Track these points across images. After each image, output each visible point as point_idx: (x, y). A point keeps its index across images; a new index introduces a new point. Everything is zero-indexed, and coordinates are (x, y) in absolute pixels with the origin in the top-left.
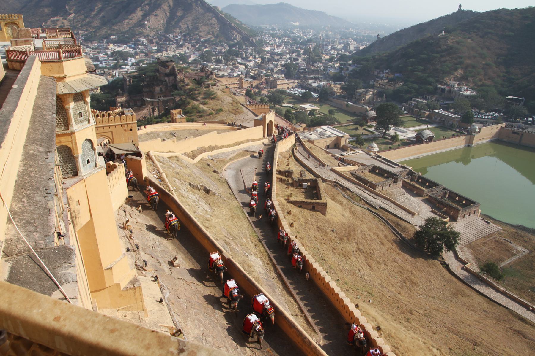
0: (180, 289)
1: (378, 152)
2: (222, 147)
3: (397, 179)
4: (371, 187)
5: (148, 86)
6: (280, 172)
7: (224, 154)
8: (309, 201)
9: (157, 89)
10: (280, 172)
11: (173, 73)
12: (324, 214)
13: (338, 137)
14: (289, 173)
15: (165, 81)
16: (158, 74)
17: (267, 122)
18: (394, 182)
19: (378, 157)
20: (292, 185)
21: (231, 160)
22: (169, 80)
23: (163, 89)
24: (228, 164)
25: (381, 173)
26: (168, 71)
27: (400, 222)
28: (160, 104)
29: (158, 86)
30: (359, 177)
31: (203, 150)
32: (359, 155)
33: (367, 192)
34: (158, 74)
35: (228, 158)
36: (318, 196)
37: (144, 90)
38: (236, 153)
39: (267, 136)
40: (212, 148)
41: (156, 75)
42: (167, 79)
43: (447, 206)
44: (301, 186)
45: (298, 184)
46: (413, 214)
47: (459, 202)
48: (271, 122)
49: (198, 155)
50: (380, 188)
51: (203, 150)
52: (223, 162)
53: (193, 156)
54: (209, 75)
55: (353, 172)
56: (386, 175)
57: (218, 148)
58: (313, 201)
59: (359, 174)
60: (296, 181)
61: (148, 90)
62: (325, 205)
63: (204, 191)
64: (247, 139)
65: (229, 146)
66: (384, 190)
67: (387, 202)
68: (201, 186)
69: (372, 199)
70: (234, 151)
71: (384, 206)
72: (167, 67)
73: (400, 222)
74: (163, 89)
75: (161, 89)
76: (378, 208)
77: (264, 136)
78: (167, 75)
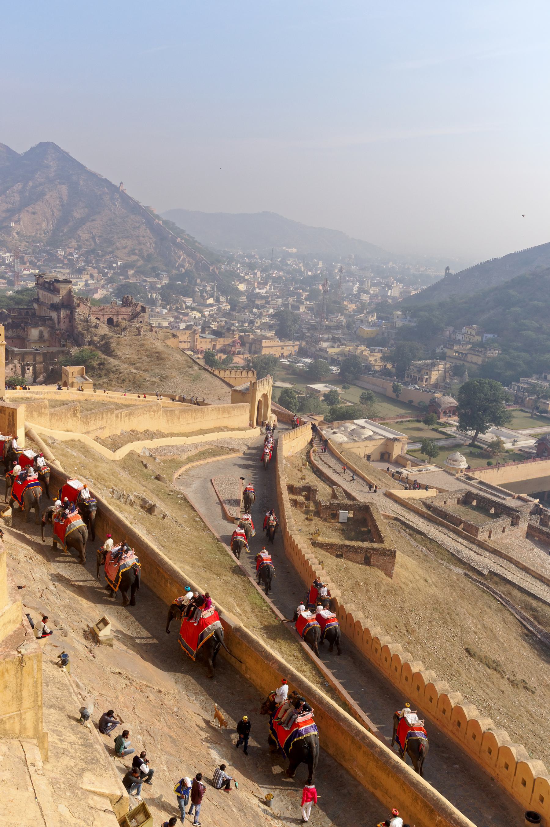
0: (122, 699)
1: (468, 469)
2: (171, 435)
3: (518, 517)
4: (469, 533)
6: (291, 489)
7: (177, 448)
9: (34, 333)
10: (291, 489)
11: (68, 304)
12: (389, 574)
13: (388, 439)
14: (309, 492)
15: (51, 319)
16: (36, 306)
18: (513, 524)
20: (317, 514)
21: (190, 460)
22: (59, 316)
23: (46, 335)
24: (184, 469)
26: (57, 299)
27: (534, 603)
28: (39, 358)
29: (36, 327)
30: (442, 511)
31: (134, 436)
32: (430, 472)
33: (460, 540)
34: (36, 306)
35: (185, 457)
36: (374, 534)
38: (200, 449)
39: (258, 424)
40: (150, 435)
41: (33, 309)
42: (54, 315)
44: (335, 516)
45: (329, 513)
48: (265, 396)
49: (123, 445)
51: (134, 436)
52: (175, 464)
53: (115, 447)
54: (138, 314)
55: (429, 502)
56: (493, 510)
57: (162, 435)
58: (365, 545)
59: (439, 504)
60: (326, 507)
62: (392, 554)
63: (142, 507)
64: (217, 425)
65: (187, 435)
66: (492, 538)
67: (501, 561)
68: (137, 497)
69: (472, 555)
70: (196, 446)
72: (56, 291)
73: (534, 603)
75: (41, 333)
76: (485, 572)
77: (251, 425)
78: (55, 307)
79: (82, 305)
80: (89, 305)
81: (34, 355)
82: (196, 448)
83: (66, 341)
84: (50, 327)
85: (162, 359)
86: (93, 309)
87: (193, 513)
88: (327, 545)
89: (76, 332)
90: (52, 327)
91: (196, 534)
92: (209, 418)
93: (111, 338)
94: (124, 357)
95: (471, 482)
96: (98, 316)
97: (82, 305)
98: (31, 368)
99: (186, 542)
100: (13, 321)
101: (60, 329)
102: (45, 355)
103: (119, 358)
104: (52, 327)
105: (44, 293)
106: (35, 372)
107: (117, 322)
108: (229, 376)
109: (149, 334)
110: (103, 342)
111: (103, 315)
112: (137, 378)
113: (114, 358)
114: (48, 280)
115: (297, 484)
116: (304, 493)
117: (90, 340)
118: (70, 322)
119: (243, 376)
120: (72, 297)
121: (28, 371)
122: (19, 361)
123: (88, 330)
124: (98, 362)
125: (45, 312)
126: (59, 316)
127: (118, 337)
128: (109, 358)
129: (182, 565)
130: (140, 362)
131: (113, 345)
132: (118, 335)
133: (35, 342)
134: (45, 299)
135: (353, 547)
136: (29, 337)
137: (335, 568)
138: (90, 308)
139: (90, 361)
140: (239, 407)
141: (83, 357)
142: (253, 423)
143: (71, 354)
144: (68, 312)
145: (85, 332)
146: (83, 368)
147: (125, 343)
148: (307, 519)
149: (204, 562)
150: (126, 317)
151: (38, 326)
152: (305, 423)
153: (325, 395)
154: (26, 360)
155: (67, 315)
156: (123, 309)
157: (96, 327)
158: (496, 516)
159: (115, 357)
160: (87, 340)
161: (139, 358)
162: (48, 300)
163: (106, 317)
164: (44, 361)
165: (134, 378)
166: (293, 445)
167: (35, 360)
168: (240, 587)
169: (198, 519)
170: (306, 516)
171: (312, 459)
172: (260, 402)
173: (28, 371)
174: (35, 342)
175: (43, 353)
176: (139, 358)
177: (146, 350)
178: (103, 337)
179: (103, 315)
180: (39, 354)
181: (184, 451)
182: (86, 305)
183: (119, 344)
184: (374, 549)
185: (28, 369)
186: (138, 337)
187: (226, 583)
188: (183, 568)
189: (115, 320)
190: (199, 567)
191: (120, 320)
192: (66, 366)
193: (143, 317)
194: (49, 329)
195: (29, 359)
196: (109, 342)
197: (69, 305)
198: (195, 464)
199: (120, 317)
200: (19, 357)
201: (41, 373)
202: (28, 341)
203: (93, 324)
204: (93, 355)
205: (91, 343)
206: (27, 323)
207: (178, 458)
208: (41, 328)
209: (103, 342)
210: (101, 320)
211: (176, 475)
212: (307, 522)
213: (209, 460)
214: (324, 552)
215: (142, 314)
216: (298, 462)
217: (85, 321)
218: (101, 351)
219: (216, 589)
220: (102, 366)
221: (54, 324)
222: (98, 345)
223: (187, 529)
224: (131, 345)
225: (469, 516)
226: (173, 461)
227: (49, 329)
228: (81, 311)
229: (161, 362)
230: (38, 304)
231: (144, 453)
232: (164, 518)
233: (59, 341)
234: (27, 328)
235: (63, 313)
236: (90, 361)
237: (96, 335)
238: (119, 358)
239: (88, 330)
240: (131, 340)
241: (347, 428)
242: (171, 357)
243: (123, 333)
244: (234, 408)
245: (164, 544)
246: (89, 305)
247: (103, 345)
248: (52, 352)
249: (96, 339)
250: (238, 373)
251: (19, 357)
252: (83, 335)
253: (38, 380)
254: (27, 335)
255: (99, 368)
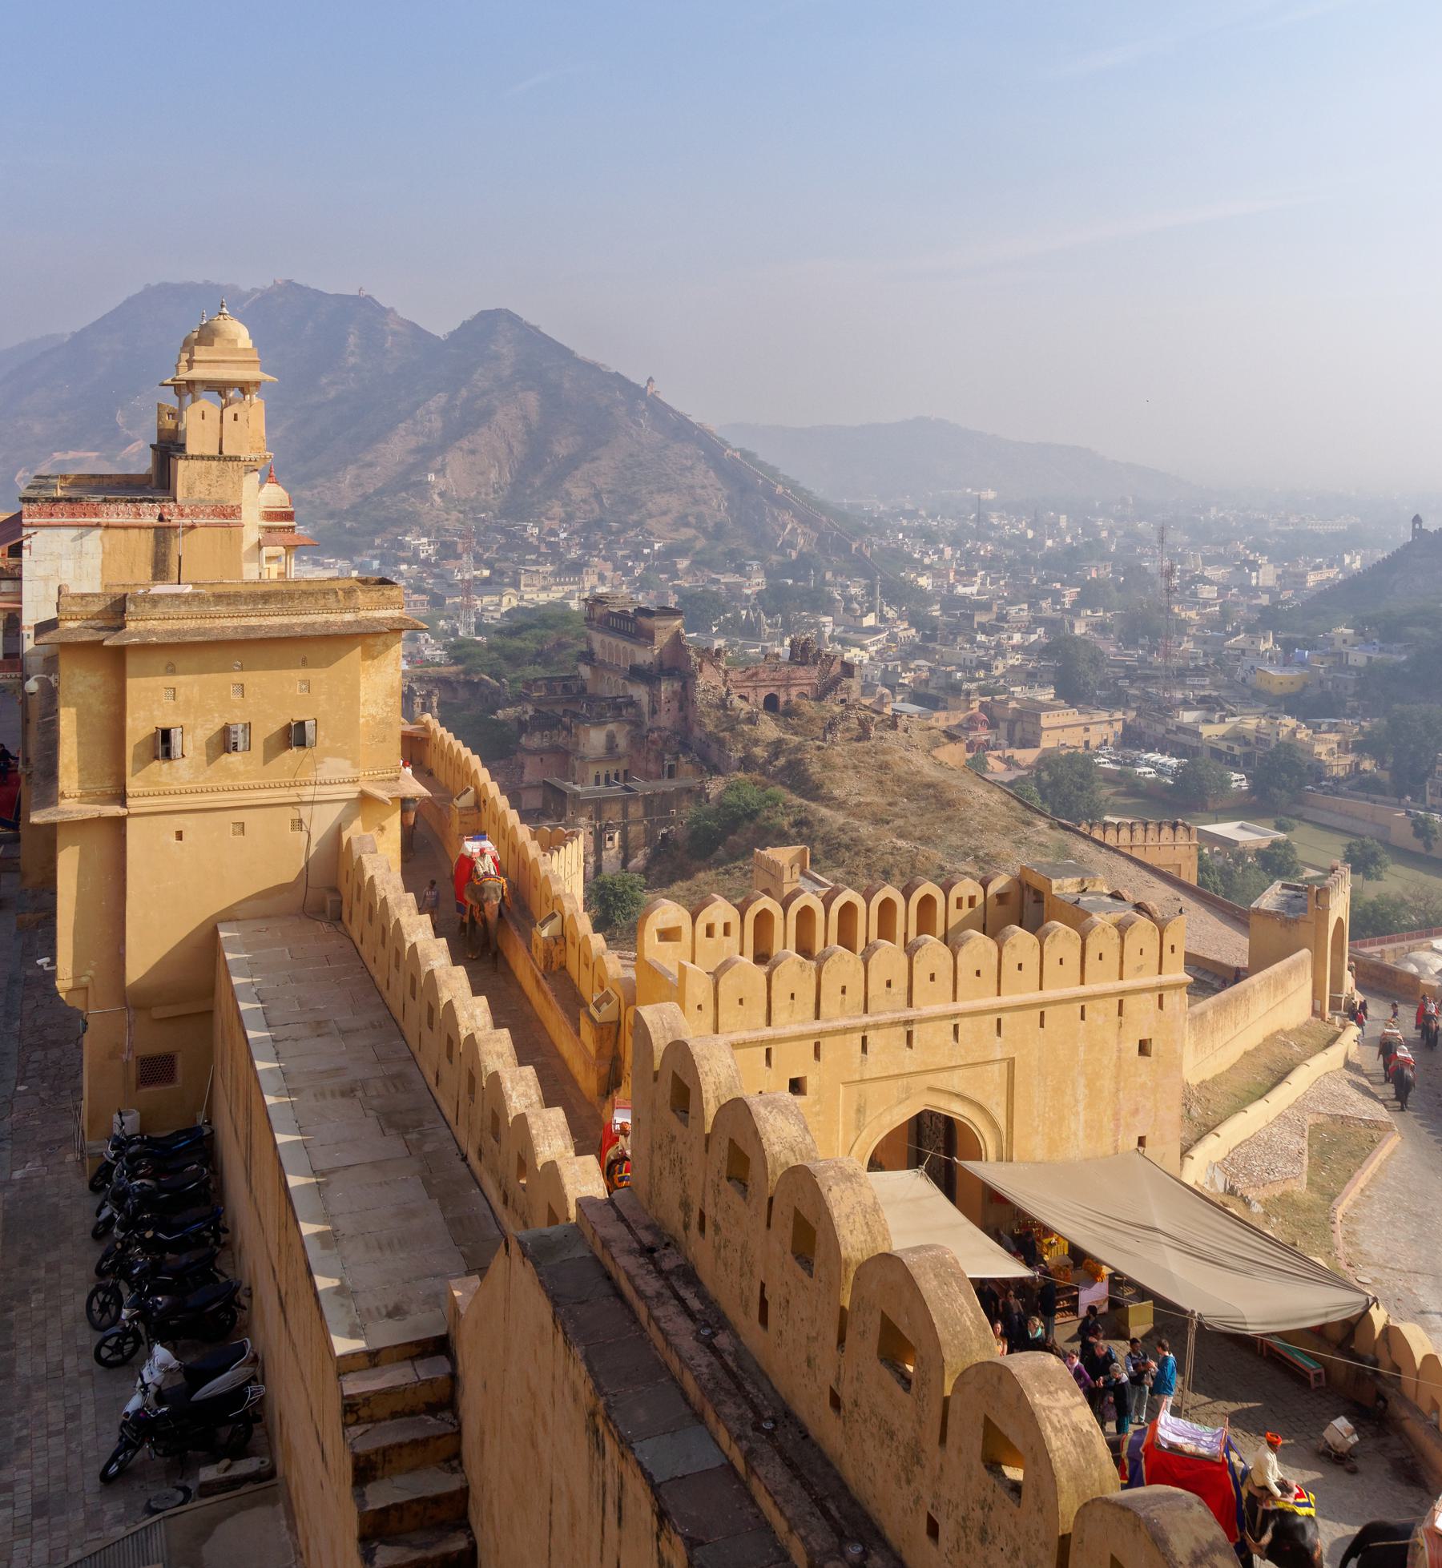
5: (544, 722)
9: (595, 739)
11: (676, 667)
15: (632, 703)
22: (654, 699)
23: (622, 742)
26: (645, 656)
28: (636, 810)
29: (600, 723)
34: (585, 671)
37: (535, 741)
42: (640, 693)
54: (836, 681)
61: (546, 744)
74: (622, 742)
75: (611, 738)
78: (637, 674)
79: (708, 669)
80: (723, 665)
81: (625, 802)
83: (677, 759)
84: (631, 722)
85: (950, 804)
86: (732, 675)
89: (697, 732)
90: (637, 724)
93: (799, 748)
94: (853, 800)
96: (743, 692)
97: (708, 669)
98: (617, 835)
100: (536, 711)
101: (659, 729)
102: (648, 801)
103: (840, 805)
104: (637, 724)
105: (608, 639)
106: (624, 845)
107: (788, 702)
108: (1127, 842)
109: (889, 735)
110: (781, 761)
111: (755, 688)
112: (918, 865)
113: (827, 806)
114: (616, 610)
117: (741, 754)
118: (681, 709)
119: (1164, 841)
120: (685, 648)
121: (609, 844)
122: (591, 818)
123: (732, 729)
124: (791, 819)
125: (611, 686)
126: (654, 699)
127: (819, 748)
128: (813, 805)
130: (896, 815)
131: (814, 768)
132: (818, 743)
133: (598, 761)
134: (611, 655)
136: (581, 748)
138: (726, 672)
139: (765, 813)
141: (747, 805)
142: (1322, 1007)
143: (708, 795)
144: (677, 686)
145: (727, 734)
146: (804, 851)
147: (839, 761)
150: (806, 689)
151: (605, 723)
153: (1259, 853)
154: (606, 816)
155: (674, 693)
156: (801, 672)
157: (752, 720)
159: (828, 800)
160: (736, 754)
161: (890, 804)
162: (618, 657)
163: (763, 693)
164: (646, 815)
165: (913, 867)
167: (625, 815)
173: (609, 844)
174: (598, 761)
175: (645, 797)
176: (890, 804)
177: (899, 780)
178: (777, 747)
179: (755, 688)
180: (636, 798)
182: (717, 667)
183: (827, 765)
185: (611, 839)
186: (867, 744)
189: (783, 699)
191: (793, 698)
192: (763, 849)
193: (849, 688)
194: (628, 728)
195: (613, 813)
196: (800, 762)
197: (676, 669)
199: (794, 692)
200: (590, 808)
201: (637, 848)
202: (582, 758)
203: (742, 715)
204: (770, 798)
205: (747, 763)
206: (575, 715)
208: (611, 727)
209: (781, 761)
210: (751, 699)
215: (846, 682)
217: (718, 707)
218: (783, 784)
220: (805, 830)
221: (640, 714)
222: (772, 769)
224: (855, 767)
227: (628, 728)
228: (708, 680)
229: (950, 812)
230: (594, 669)
231: (1212, 1182)
233: (660, 757)
234: (577, 728)
235: (666, 688)
236: (765, 813)
237: (756, 742)
238: (840, 805)
239: (732, 729)
240: (853, 753)
241: (1426, 965)
242: (969, 798)
243: (829, 736)
246: (723, 665)
247: (782, 769)
248: (664, 793)
249: (759, 752)
250: (1150, 834)
251: (590, 808)
252: (721, 743)
253: (632, 863)
254: (577, 744)
255: (799, 834)
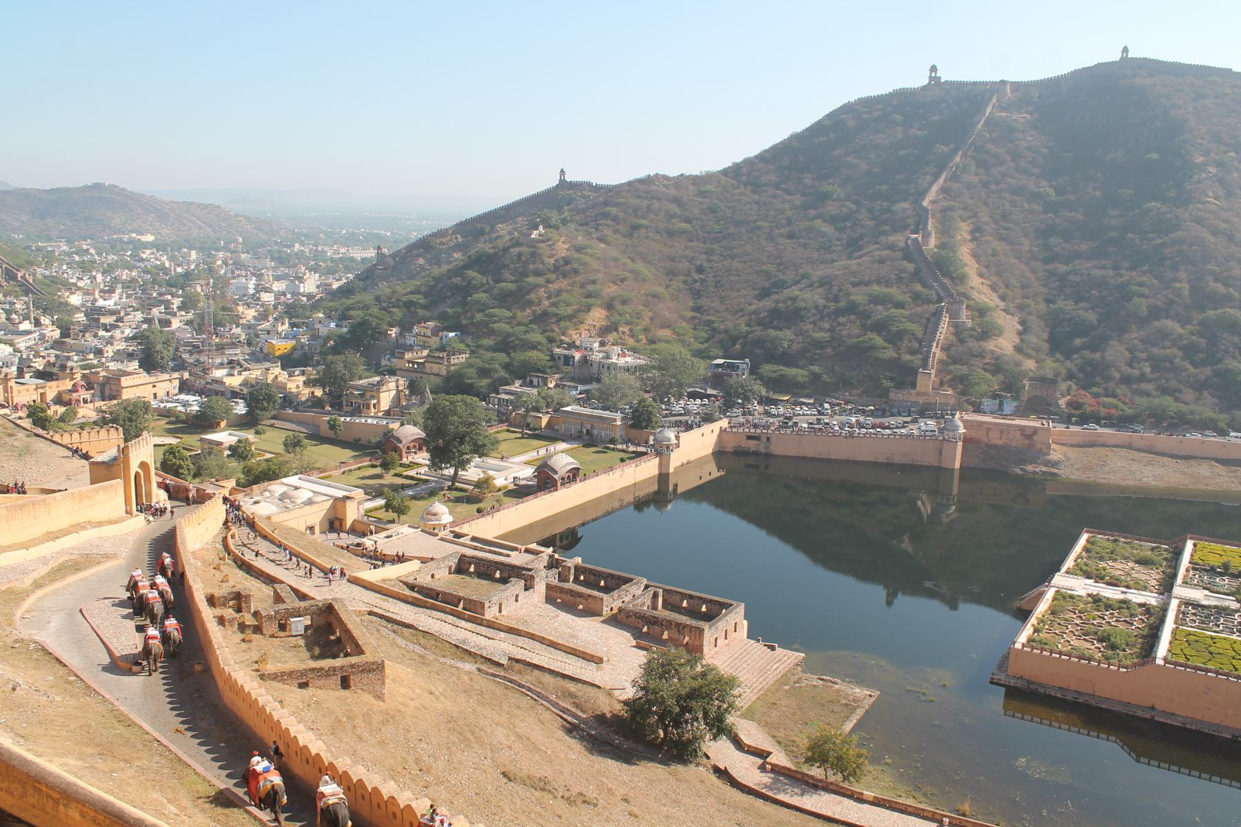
1: (454, 524)
3: (532, 577)
4: (472, 611)
6: (211, 601)
7: (13, 569)
8: (326, 663)
12: (380, 697)
13: (336, 499)
17: (134, 468)
19: (458, 536)
20: (258, 629)
21: (38, 585)
24: (31, 600)
25: (486, 571)
27: (572, 687)
30: (431, 590)
32: (402, 536)
33: (463, 623)
35: (28, 581)
38: (53, 564)
43: (669, 624)
46: (598, 661)
47: (693, 613)
48: (143, 465)
50: (495, 609)
55: (410, 580)
58: (339, 662)
59: (424, 580)
60: (270, 618)
65: (26, 546)
66: (504, 612)
67: (522, 641)
69: (483, 641)
70: (44, 560)
71: (521, 654)
76: (504, 661)
82: (45, 564)
87: (62, 671)
88: (283, 674)
91: (73, 702)
92: (60, 512)
95: (461, 540)
99: (62, 720)
115: (219, 592)
116: (231, 603)
129: (64, 760)
135: (321, 669)
137: (300, 705)
140: (105, 488)
148: (243, 640)
149: (98, 745)
152: (210, 497)
153: (231, 448)
158: (504, 581)
166: (200, 531)
168: (165, 771)
169: (72, 678)
170: (241, 636)
171: (232, 547)
172: (137, 475)
181: (25, 572)
184: (352, 666)
187: (141, 770)
188: (66, 764)
190: (92, 755)
198: (48, 589)
207: (18, 585)
211: (19, 614)
212: (244, 646)
213: (71, 579)
214: (280, 685)
216: (212, 557)
219: (128, 784)
223: (58, 698)
225: (471, 587)
226: (10, 591)
232: (14, 689)
244: (97, 491)
245: (23, 732)
